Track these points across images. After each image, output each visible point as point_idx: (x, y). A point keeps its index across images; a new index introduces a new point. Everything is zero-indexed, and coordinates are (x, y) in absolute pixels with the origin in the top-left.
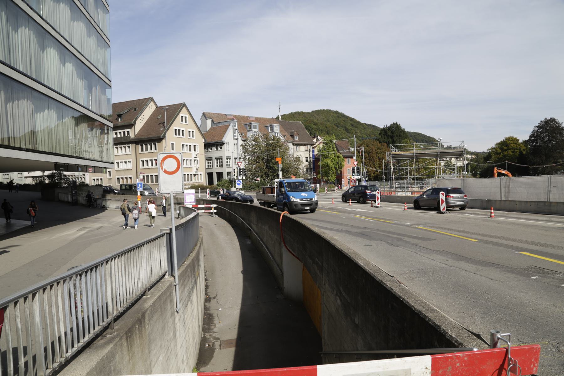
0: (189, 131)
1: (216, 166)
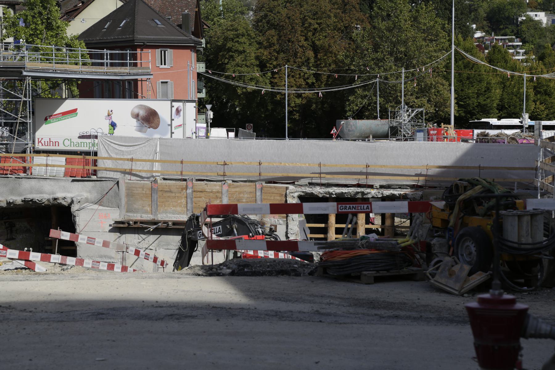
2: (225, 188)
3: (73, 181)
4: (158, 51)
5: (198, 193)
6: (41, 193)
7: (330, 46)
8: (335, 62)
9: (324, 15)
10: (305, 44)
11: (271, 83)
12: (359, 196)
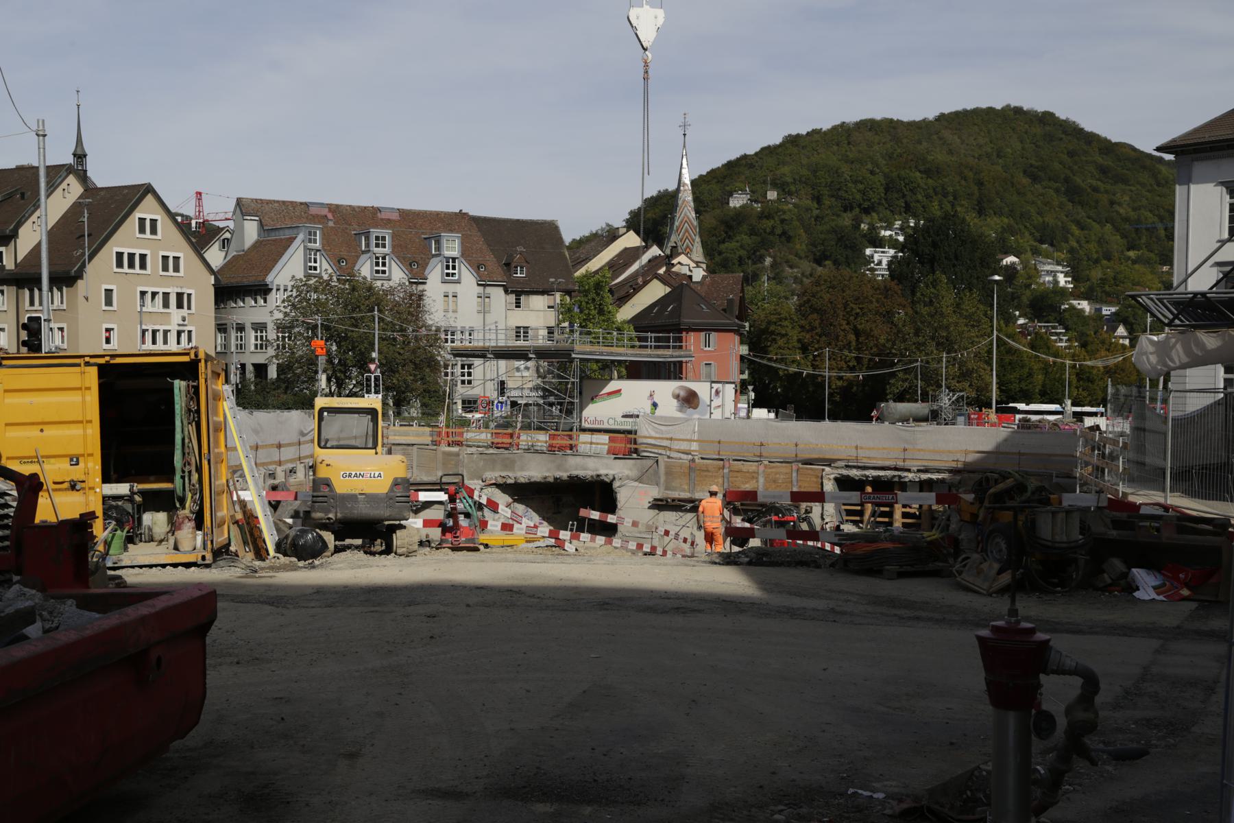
0: (165, 258)
1: (252, 348)
2: (761, 468)
3: (615, 458)
4: (703, 334)
5: (735, 474)
6: (585, 469)
7: (871, 330)
8: (876, 346)
9: (866, 301)
10: (847, 327)
11: (812, 365)
12: (896, 479)
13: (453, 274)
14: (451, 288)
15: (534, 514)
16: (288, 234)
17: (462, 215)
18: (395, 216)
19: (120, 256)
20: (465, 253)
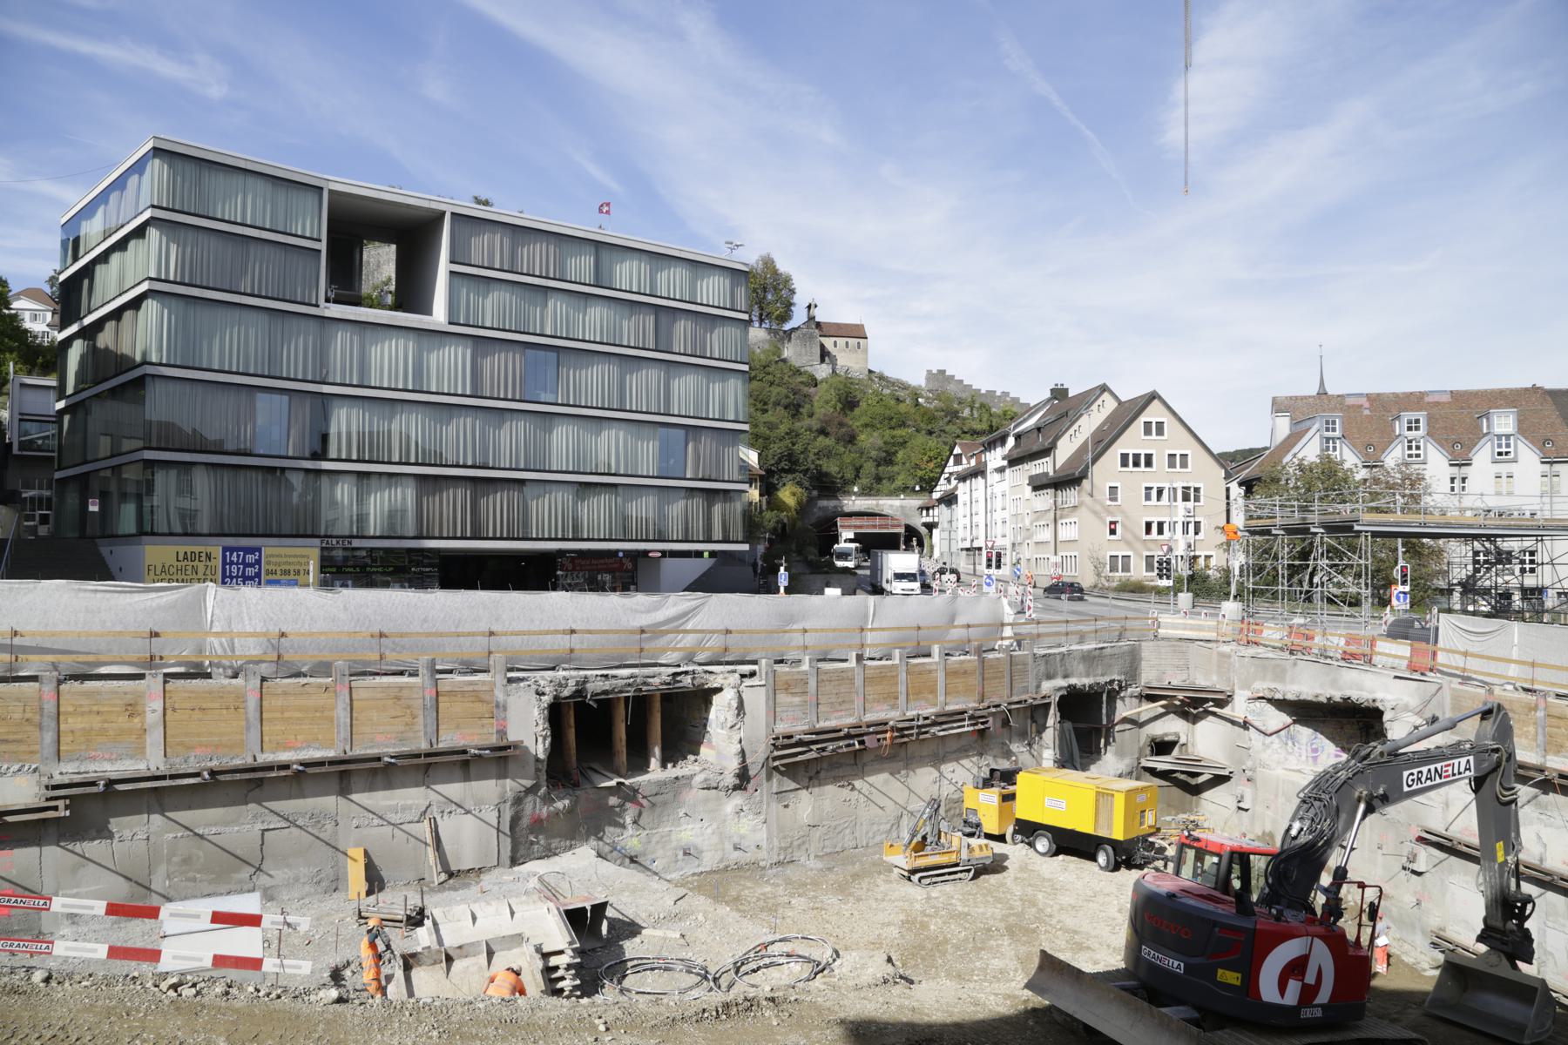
0: (1172, 456)
3: (1396, 677)
6: (1361, 690)
13: (1507, 453)
14: (1504, 469)
15: (1327, 742)
16: (1308, 423)
17: (1535, 389)
18: (1446, 398)
19: (1124, 457)
20: (1524, 429)
